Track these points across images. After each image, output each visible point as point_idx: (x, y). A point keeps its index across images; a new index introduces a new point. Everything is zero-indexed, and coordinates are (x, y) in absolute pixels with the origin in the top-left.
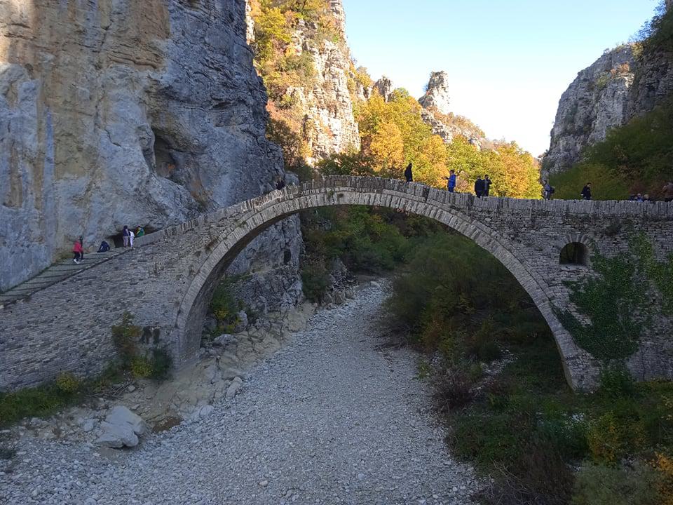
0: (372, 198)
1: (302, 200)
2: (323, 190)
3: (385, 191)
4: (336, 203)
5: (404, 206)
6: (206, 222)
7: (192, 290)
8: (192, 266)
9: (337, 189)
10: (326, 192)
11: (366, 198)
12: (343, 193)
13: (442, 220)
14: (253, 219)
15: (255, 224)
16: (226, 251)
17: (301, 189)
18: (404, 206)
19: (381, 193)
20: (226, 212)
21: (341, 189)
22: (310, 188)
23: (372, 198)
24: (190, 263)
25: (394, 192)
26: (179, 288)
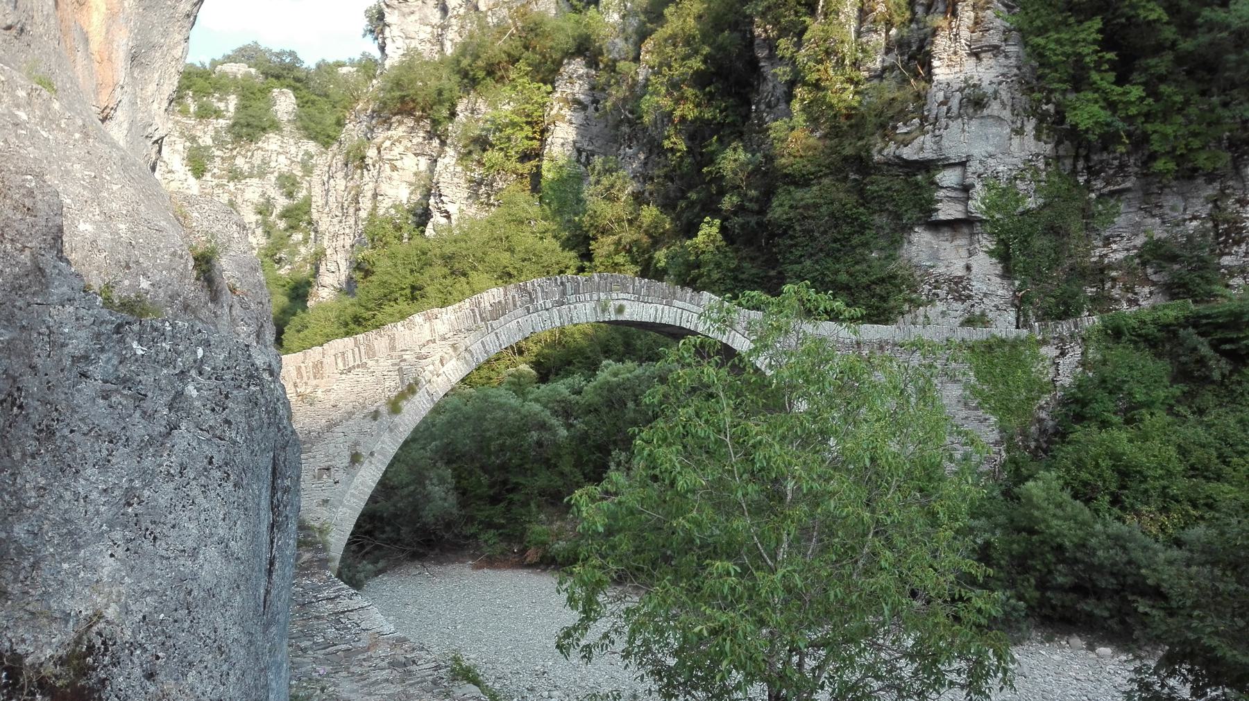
0: (660, 312)
1: (564, 312)
2: (595, 297)
3: (676, 303)
4: (613, 318)
5: (696, 326)
6: (393, 348)
7: (353, 495)
8: (356, 444)
9: (614, 296)
10: (599, 300)
11: (652, 311)
12: (625, 302)
13: (735, 346)
14: (482, 343)
15: (486, 352)
16: (430, 406)
17: (564, 293)
18: (696, 326)
19: (669, 304)
20: (433, 330)
21: (622, 295)
22: (576, 292)
23: (660, 312)
24: (353, 436)
25: (686, 305)
26: (325, 495)
